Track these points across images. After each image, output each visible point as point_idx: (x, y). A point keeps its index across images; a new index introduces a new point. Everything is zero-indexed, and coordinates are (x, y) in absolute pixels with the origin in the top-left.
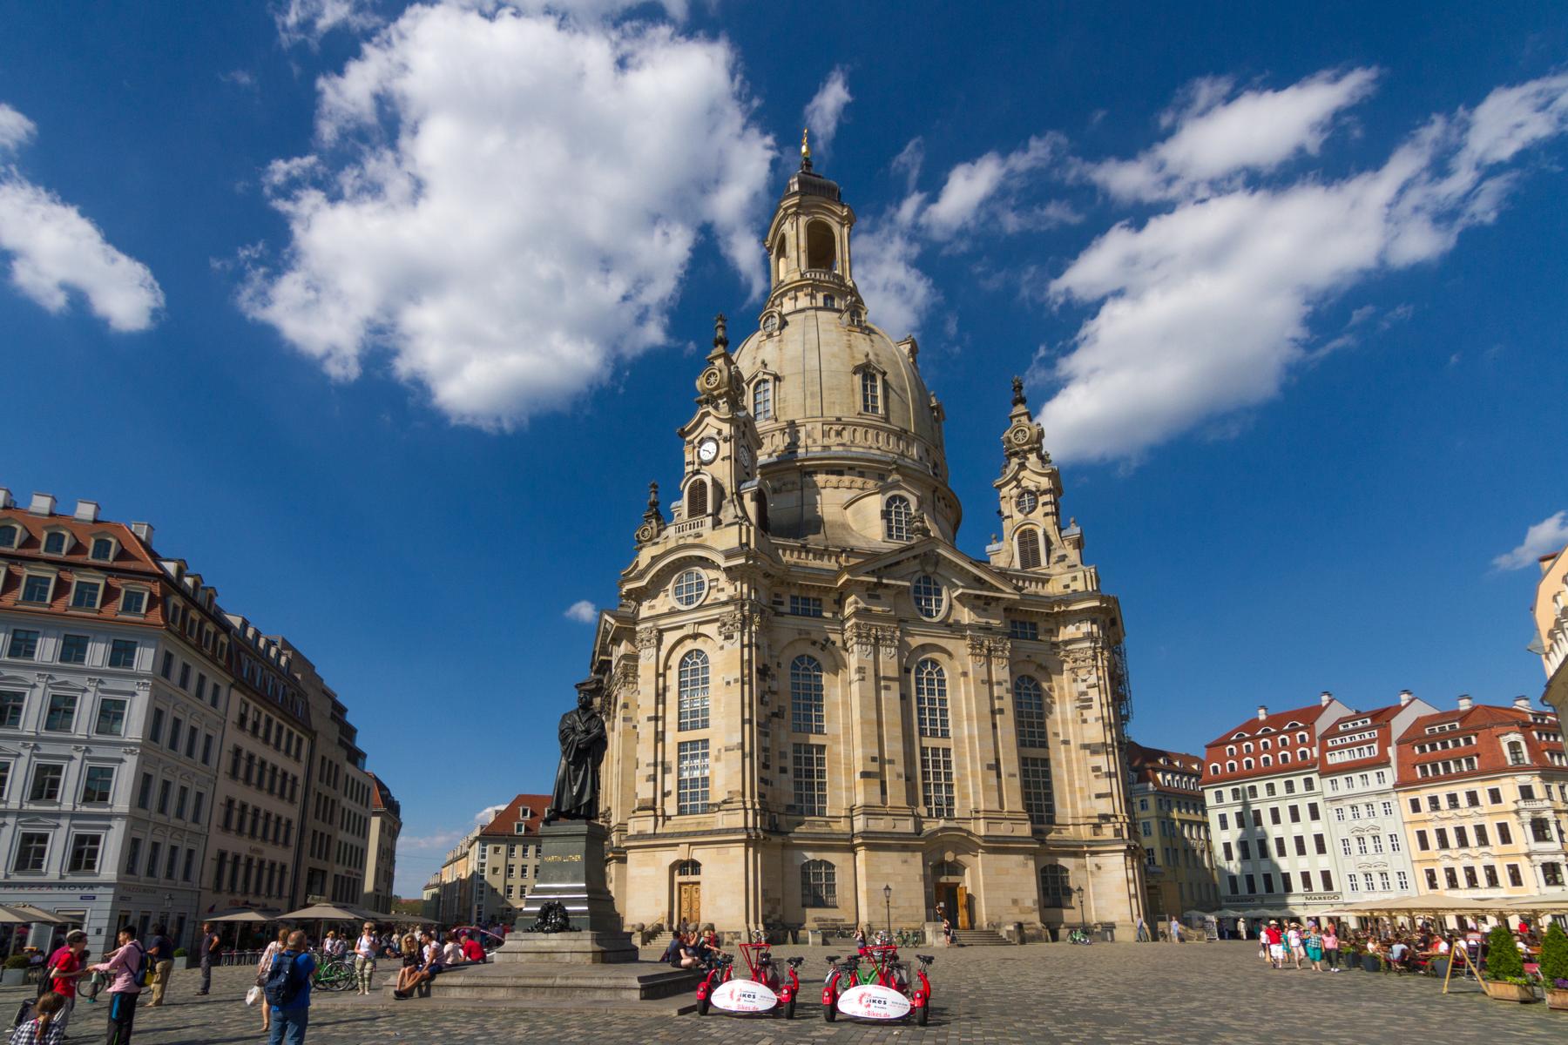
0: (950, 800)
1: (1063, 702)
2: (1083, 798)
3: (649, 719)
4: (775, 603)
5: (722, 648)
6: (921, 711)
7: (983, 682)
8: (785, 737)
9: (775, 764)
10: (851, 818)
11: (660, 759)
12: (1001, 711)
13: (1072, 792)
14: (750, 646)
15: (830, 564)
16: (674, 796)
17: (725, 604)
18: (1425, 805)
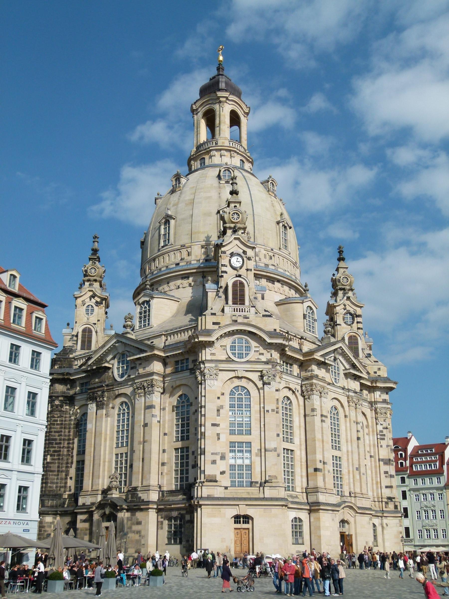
3: (213, 425)
5: (261, 388)
16: (227, 475)
17: (267, 363)
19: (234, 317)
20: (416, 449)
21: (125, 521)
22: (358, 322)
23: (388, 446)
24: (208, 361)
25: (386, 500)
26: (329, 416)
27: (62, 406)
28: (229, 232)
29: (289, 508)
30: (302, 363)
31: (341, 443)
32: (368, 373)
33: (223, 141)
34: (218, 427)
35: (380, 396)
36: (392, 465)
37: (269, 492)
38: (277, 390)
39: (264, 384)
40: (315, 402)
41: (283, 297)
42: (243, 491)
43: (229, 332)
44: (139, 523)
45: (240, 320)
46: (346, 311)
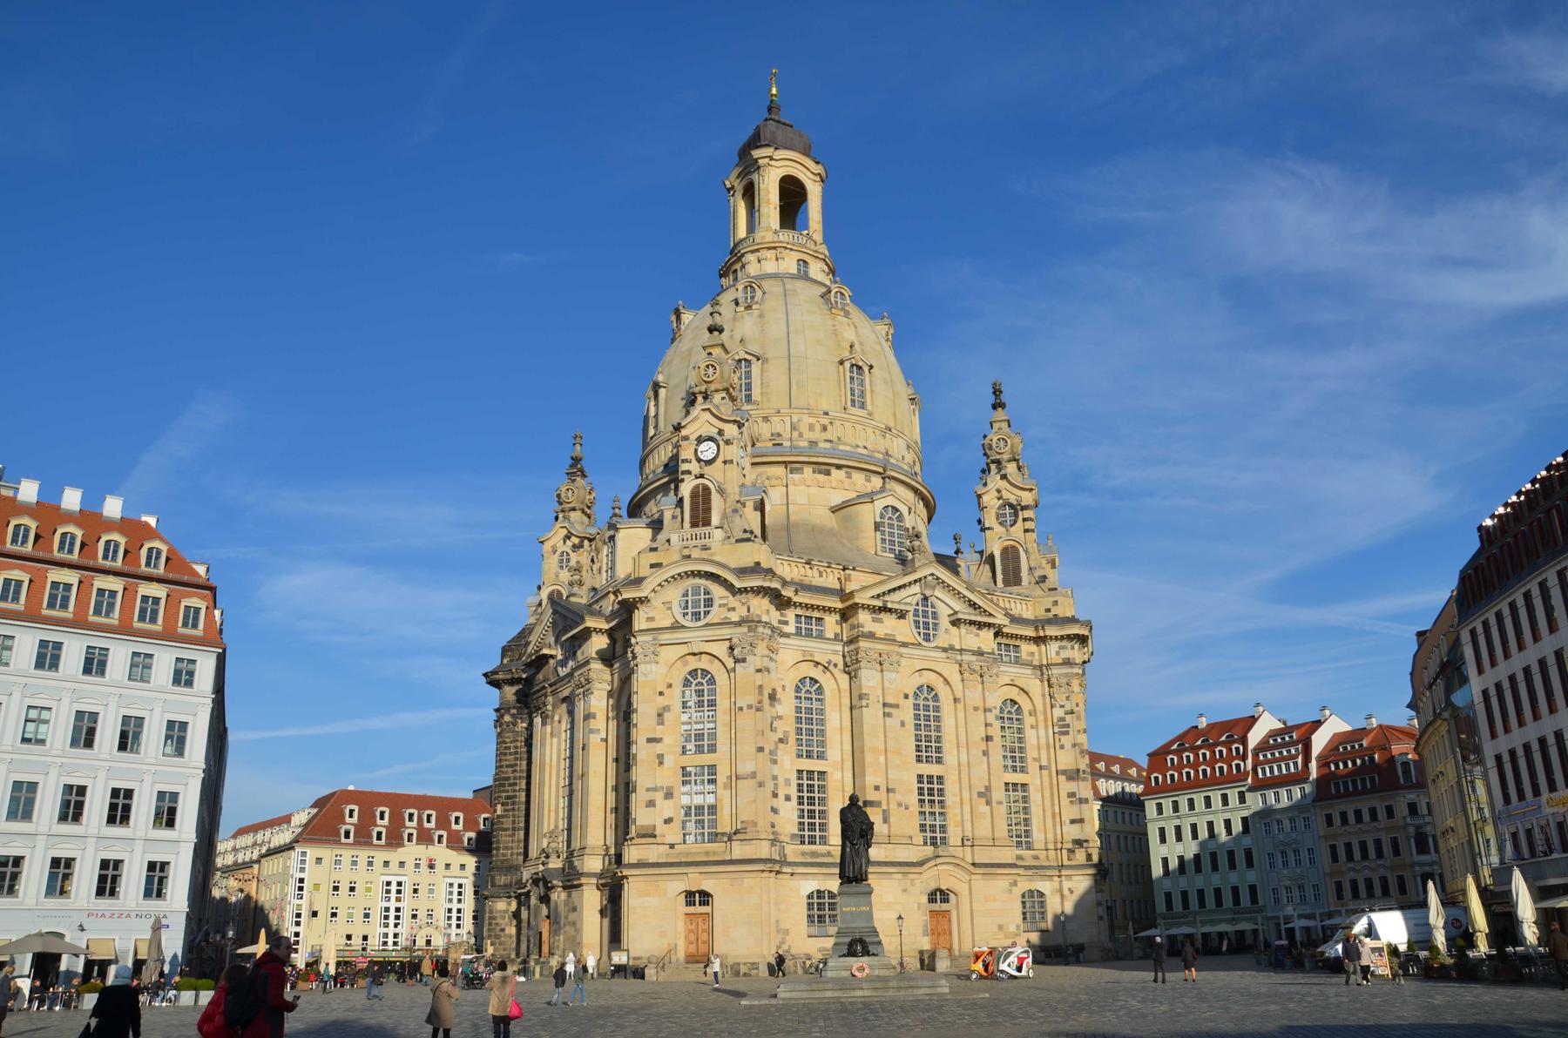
3: (650, 740)
4: (780, 622)
18: (1337, 820)
20: (1273, 734)
21: (561, 907)
23: (1074, 745)
25: (1070, 846)
26: (911, 700)
27: (515, 724)
28: (700, 398)
31: (945, 749)
35: (1058, 653)
36: (1084, 779)
37: (738, 850)
38: (759, 671)
39: (737, 661)
40: (864, 681)
41: (854, 495)
44: (574, 909)
45: (696, 554)
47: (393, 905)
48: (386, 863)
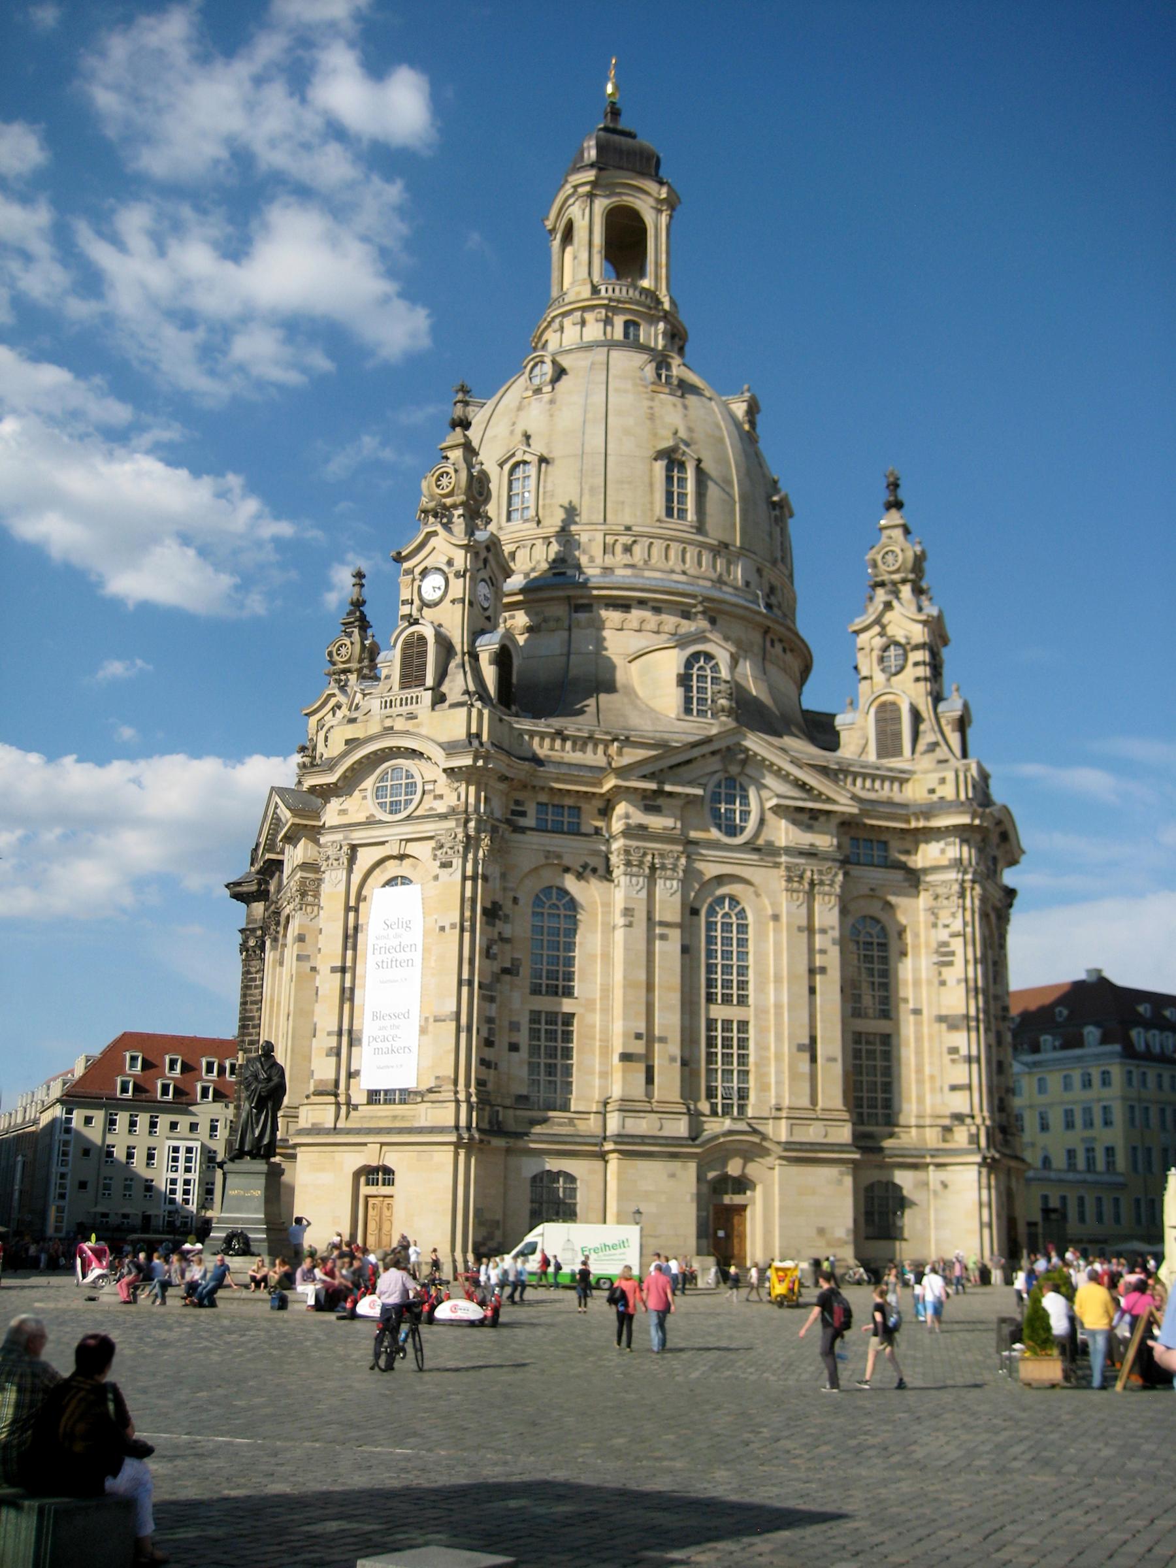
0: (743, 1094)
1: (917, 955)
2: (933, 1090)
3: (334, 970)
4: (514, 813)
5: (436, 878)
6: (710, 969)
7: (800, 929)
8: (520, 1002)
9: (502, 1041)
10: (604, 1114)
11: (345, 1027)
12: (823, 970)
13: (920, 1082)
14: (474, 878)
15: (593, 757)
19: (389, 720)
22: (916, 664)
23: (959, 981)
24: (331, 827)
25: (947, 1122)
29: (508, 1151)
30: (609, 800)
31: (751, 986)
32: (854, 797)
33: (577, 289)
34: (348, 976)
35: (943, 851)
42: (388, 1113)
43: (367, 757)
46: (884, 639)
47: (180, 1176)
48: (173, 1126)
